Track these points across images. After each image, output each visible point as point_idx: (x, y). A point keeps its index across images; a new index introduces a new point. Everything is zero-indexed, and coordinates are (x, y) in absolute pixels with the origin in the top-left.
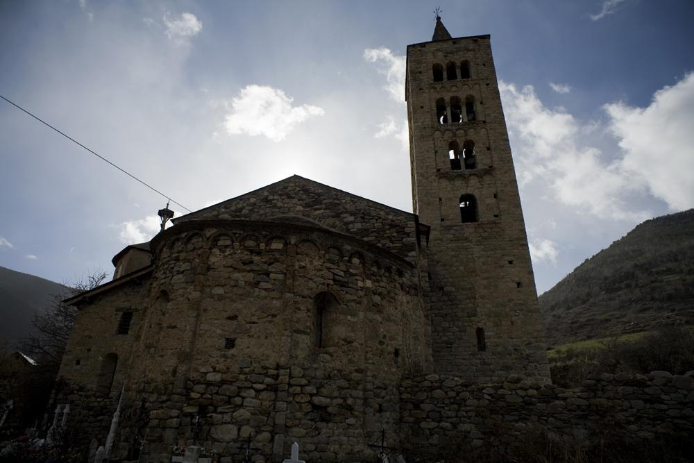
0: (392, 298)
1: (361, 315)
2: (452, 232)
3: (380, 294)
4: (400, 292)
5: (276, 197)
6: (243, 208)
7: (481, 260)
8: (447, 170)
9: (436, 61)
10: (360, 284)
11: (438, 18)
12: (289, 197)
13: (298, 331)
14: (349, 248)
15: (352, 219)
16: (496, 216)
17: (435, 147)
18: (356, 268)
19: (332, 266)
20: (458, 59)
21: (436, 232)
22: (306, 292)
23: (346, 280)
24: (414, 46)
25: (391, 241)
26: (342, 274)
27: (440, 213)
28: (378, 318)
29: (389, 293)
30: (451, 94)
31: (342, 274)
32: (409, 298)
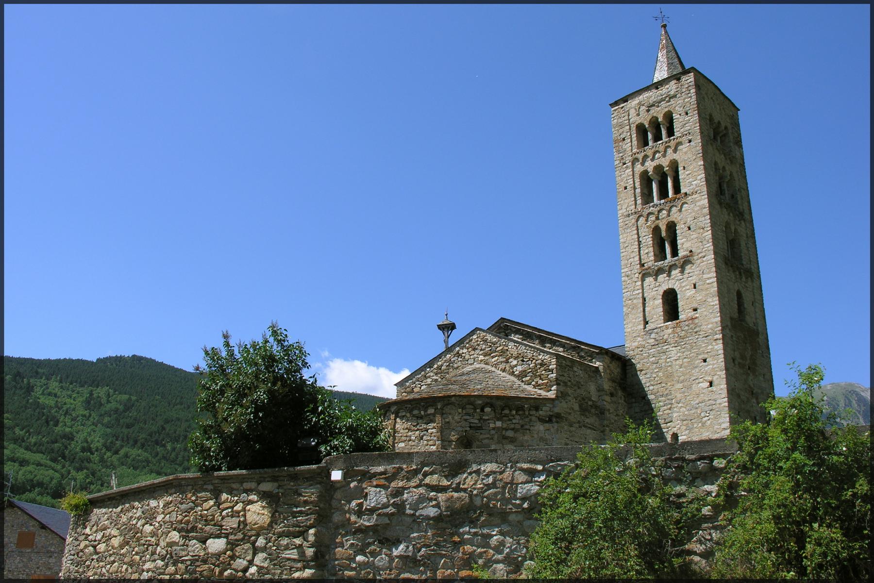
2: (653, 336)
3: (513, 429)
4: (539, 423)
5: (465, 351)
6: (442, 365)
7: (678, 362)
8: (650, 264)
9: (638, 120)
10: (492, 425)
12: (474, 349)
15: (515, 362)
16: (695, 310)
17: (639, 238)
19: (468, 417)
20: (659, 113)
21: (639, 339)
25: (541, 379)
26: (476, 421)
29: (522, 426)
30: (654, 164)
31: (476, 421)
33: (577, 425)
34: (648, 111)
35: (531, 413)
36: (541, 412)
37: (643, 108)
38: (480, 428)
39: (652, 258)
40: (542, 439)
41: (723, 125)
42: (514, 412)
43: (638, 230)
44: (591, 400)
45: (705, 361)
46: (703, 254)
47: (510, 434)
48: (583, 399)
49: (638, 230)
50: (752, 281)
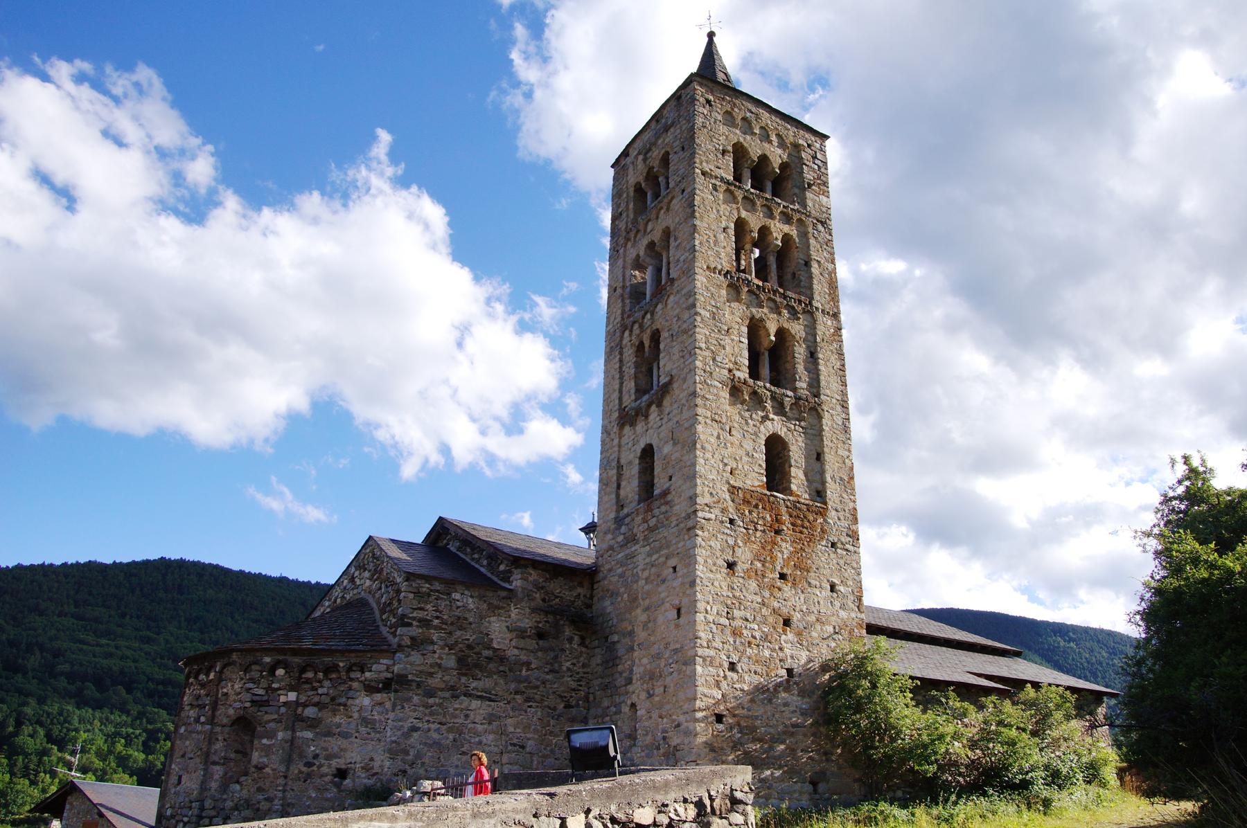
0: (340, 704)
1: (280, 735)
3: (316, 705)
4: (363, 693)
10: (283, 699)
13: (215, 763)
14: (267, 660)
18: (279, 681)
19: (251, 685)
21: (610, 536)
22: (225, 721)
23: (265, 698)
24: (618, 161)
27: (618, 496)
28: (309, 734)
29: (333, 699)
31: (261, 692)
32: (378, 697)
33: (447, 694)
34: (645, 160)
35: (353, 675)
36: (368, 674)
37: (641, 157)
38: (266, 703)
39: (633, 397)
40: (365, 721)
42: (321, 675)
43: (621, 354)
44: (489, 648)
45: (674, 568)
47: (310, 712)
48: (470, 647)
49: (621, 354)
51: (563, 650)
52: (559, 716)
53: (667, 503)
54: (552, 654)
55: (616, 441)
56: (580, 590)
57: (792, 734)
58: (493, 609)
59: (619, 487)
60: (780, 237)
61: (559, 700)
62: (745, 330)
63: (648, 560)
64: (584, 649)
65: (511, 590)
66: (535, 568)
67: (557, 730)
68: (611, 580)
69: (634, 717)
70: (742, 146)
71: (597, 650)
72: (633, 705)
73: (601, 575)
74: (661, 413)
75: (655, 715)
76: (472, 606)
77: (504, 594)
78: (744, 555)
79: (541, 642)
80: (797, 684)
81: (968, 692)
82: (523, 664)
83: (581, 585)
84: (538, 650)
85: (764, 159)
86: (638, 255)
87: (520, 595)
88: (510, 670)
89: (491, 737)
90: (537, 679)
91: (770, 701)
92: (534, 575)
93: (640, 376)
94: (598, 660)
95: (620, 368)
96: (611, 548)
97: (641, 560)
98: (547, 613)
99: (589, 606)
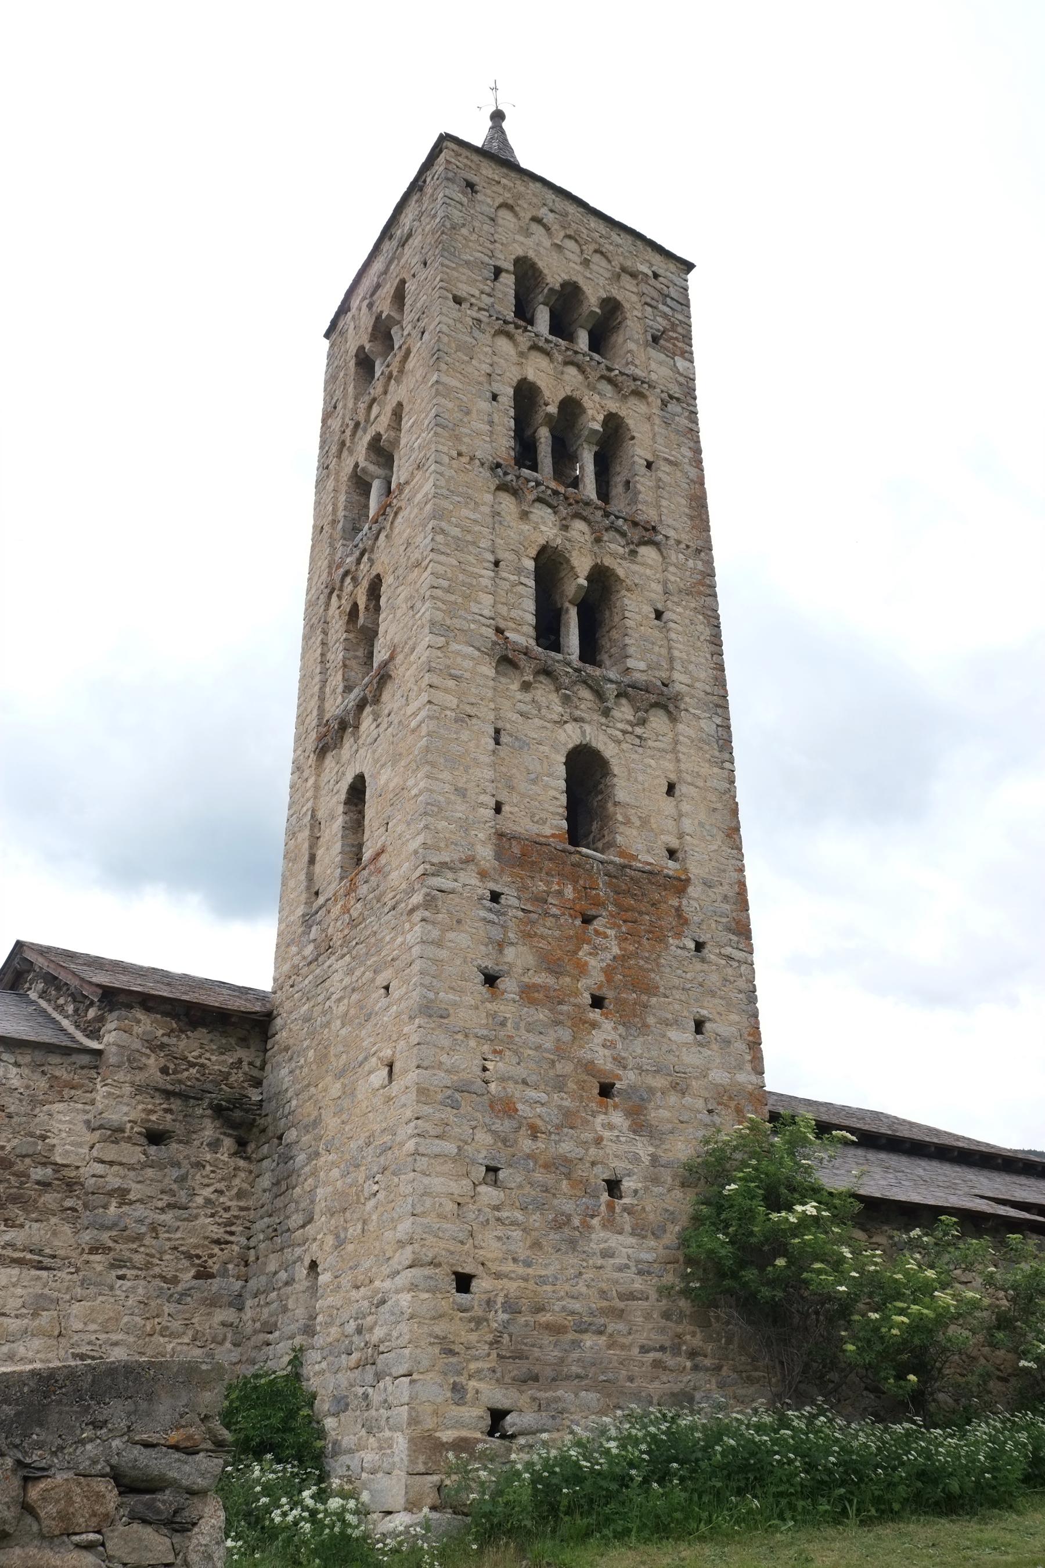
11: (498, 116)
21: (294, 949)
27: (310, 878)
34: (370, 306)
41: (593, 297)
45: (387, 988)
46: (411, 643)
49: (325, 633)
50: (673, 719)
51: (199, 1165)
52: (184, 1294)
53: (379, 871)
54: (175, 1173)
55: (311, 781)
56: (241, 1053)
57: (619, 1314)
58: (59, 1089)
59: (312, 860)
60: (601, 417)
61: (186, 1263)
62: (530, 565)
63: (347, 981)
64: (242, 1163)
65: (99, 1053)
66: (148, 1009)
67: (176, 1325)
68: (287, 1030)
69: (313, 1290)
70: (533, 266)
71: (265, 1163)
72: (313, 1265)
73: (279, 1021)
74: (376, 716)
75: (345, 1281)
76: (15, 1082)
77: (85, 1059)
78: (518, 958)
79: (152, 1150)
80: (628, 1210)
81: (973, 1222)
82: (110, 1194)
83: (244, 1042)
84: (144, 1166)
85: (571, 292)
86: (357, 465)
87: (113, 1060)
88: (86, 1206)
89: (37, 1343)
90: (140, 1221)
91: (573, 1243)
92: (145, 1024)
93: (353, 663)
94: (266, 1181)
95: (322, 655)
96: (296, 970)
97: (338, 982)
98: (168, 1094)
99: (258, 1083)
